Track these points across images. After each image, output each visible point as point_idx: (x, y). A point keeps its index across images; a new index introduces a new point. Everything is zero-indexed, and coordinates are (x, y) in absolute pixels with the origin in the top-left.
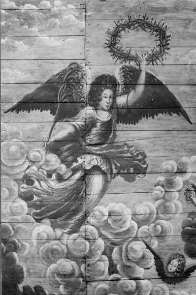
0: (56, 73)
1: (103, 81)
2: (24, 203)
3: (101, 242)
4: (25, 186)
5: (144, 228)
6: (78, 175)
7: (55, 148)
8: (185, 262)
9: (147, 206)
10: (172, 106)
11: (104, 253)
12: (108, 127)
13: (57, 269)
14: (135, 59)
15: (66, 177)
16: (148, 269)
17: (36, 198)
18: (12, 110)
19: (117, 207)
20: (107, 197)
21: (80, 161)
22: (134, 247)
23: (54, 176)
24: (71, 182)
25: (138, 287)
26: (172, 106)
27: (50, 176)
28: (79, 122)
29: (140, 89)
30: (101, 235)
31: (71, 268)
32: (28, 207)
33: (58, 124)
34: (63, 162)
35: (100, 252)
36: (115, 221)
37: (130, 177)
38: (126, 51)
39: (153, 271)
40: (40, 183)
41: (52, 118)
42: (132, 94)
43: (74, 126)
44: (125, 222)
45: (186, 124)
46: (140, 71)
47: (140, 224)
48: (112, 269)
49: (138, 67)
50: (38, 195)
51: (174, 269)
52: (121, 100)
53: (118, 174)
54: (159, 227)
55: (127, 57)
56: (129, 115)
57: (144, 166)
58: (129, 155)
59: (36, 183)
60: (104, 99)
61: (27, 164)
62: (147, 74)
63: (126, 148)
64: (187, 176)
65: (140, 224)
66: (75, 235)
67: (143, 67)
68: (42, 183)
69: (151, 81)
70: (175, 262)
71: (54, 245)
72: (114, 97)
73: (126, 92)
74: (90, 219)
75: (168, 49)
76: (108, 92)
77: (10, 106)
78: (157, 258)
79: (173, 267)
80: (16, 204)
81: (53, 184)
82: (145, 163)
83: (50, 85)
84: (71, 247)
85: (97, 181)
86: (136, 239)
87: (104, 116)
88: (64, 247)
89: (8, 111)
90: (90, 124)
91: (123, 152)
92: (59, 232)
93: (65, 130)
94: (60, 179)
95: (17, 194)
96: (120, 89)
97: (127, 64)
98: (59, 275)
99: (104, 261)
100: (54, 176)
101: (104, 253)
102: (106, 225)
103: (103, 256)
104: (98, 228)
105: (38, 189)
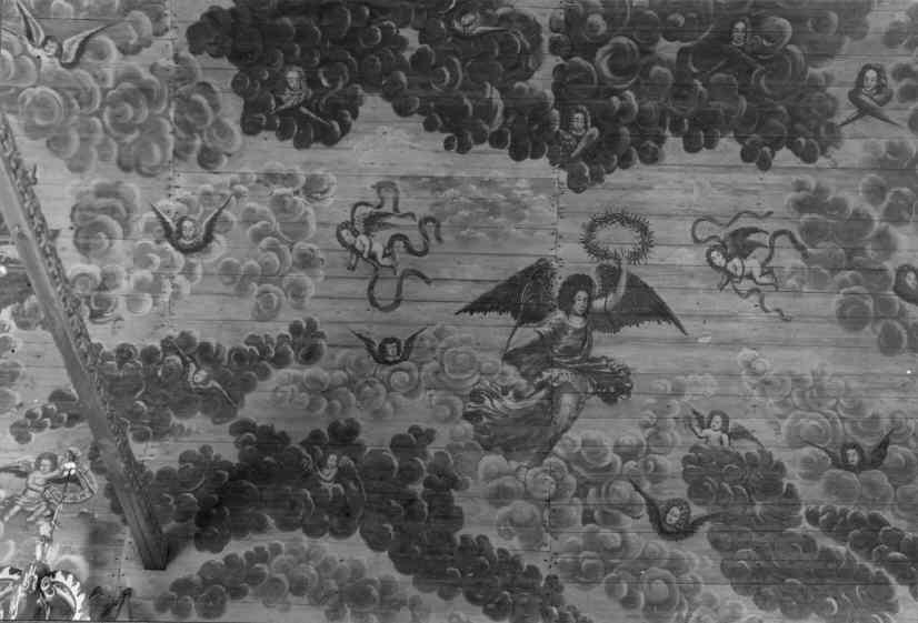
0: (520, 269)
1: (579, 282)
2: (468, 425)
3: (571, 479)
4: (472, 404)
5: (631, 464)
6: (542, 393)
7: (510, 357)
8: (689, 513)
9: (633, 435)
10: (661, 313)
11: (576, 495)
12: (585, 336)
13: (510, 513)
14: (616, 257)
15: (528, 394)
16: (638, 518)
17: (485, 420)
18: (465, 310)
19: (593, 435)
20: (580, 421)
21: (546, 375)
22: (618, 488)
23: (511, 393)
24: (533, 402)
25: (624, 543)
26: (661, 313)
27: (505, 393)
28: (545, 329)
29: (622, 290)
30: (571, 470)
31: (528, 516)
32: (475, 430)
33: (519, 329)
34: (524, 375)
35: (570, 494)
36: (590, 454)
37: (609, 399)
38: (601, 247)
39: (645, 519)
40: (492, 401)
41: (513, 322)
42: (611, 297)
43: (539, 332)
44: (605, 455)
45: (679, 334)
46: (620, 270)
47: (626, 457)
48: (588, 518)
49: (617, 266)
50: (488, 416)
51: (675, 519)
52: (599, 304)
53: (594, 394)
54: (651, 463)
55: (605, 255)
56: (612, 321)
57: (628, 385)
58: (608, 370)
59: (488, 402)
60: (578, 302)
61: (477, 377)
62: (628, 274)
63: (604, 363)
64: (686, 399)
65: (626, 457)
66: (537, 469)
67: (624, 265)
68: (495, 402)
69: (633, 281)
70: (676, 510)
71: (509, 482)
72: (590, 300)
73: (605, 295)
74: (557, 449)
75: (652, 246)
76: (582, 294)
77: (462, 306)
78: (651, 503)
79: (674, 517)
80: (459, 428)
81: (509, 402)
82: (628, 381)
83: (513, 284)
84: (530, 486)
85: (567, 399)
86: (620, 477)
87: (577, 323)
88: (521, 485)
89: (460, 312)
90: (560, 329)
91: (600, 367)
92: (514, 465)
93: (528, 334)
94: (518, 397)
95: (461, 414)
96: (597, 289)
97: (605, 262)
98: (512, 521)
99: (575, 505)
100: (511, 393)
101: (576, 495)
102: (579, 460)
103: (575, 499)
104: (567, 462)
105: (489, 409)
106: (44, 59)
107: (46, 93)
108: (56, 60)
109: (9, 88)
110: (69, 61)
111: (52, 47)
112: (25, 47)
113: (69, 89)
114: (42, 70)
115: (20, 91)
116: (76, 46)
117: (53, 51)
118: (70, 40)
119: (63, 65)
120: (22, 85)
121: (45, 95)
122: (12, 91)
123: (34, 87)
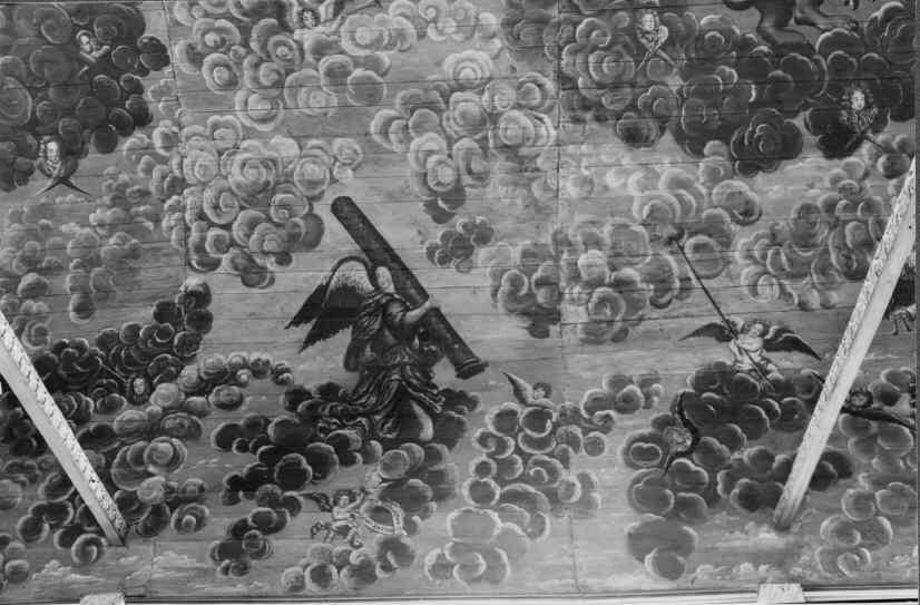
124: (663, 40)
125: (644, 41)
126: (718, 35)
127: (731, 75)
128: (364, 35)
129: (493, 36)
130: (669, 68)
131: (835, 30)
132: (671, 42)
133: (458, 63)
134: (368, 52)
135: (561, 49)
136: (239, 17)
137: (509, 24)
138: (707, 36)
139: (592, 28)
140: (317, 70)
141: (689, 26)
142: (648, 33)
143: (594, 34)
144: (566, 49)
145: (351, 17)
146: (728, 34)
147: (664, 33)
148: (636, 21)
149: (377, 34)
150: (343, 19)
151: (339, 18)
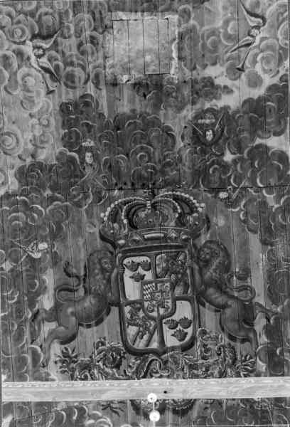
106: (261, 35)
107: (281, 32)
108: (262, 28)
109: (279, 53)
110: (261, 21)
111: (254, 32)
112: (255, 47)
113: (278, 20)
114: (268, 36)
115: (281, 48)
116: (253, 18)
117: (256, 31)
118: (250, 22)
119: (264, 25)
120: (277, 48)
121: (283, 32)
122: (281, 51)
123: (278, 40)
124: (33, 256)
125: (32, 244)
126: (37, 287)
127: (13, 299)
128: (31, 81)
129: (33, 156)
130: (16, 261)
131: (42, 354)
132: (32, 260)
133: (16, 135)
134: (20, 82)
135: (26, 196)
136: (39, 13)
137: (41, 166)
138: (36, 281)
139: (40, 213)
140: (7, 50)
141: (43, 270)
142: (37, 247)
143: (35, 215)
144: (26, 199)
145: (40, 75)
146: (38, 294)
147: (37, 255)
148: (43, 240)
149: (31, 89)
150: (40, 71)
151: (40, 69)
